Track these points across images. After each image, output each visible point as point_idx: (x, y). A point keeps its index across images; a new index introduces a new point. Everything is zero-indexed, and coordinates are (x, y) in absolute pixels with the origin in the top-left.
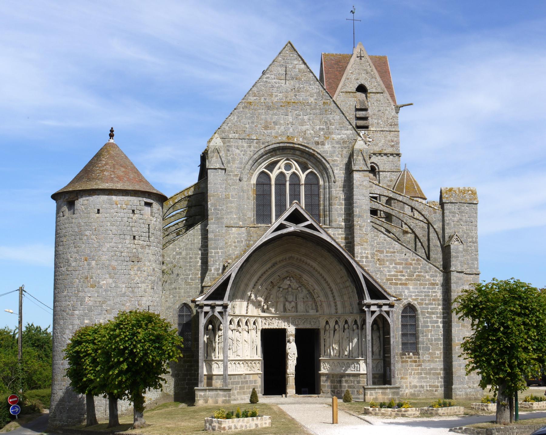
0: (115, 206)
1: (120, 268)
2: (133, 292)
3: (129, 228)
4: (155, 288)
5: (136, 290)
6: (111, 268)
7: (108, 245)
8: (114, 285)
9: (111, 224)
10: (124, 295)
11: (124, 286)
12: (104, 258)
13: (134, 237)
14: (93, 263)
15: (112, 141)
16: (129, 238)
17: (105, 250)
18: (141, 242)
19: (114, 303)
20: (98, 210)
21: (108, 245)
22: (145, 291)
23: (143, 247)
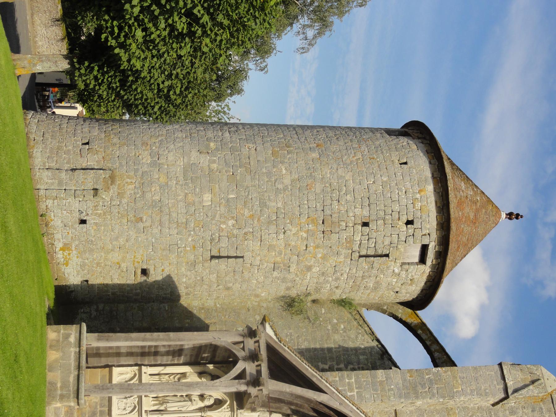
0: (416, 189)
1: (311, 197)
2: (269, 223)
3: (382, 213)
4: (275, 274)
5: (273, 228)
6: (310, 181)
7: (348, 176)
8: (280, 186)
9: (386, 182)
10: (263, 205)
11: (280, 205)
12: (327, 171)
13: (366, 224)
14: (315, 155)
15: (504, 216)
16: (363, 213)
17: (340, 172)
18: (358, 238)
19: (247, 187)
20: (406, 163)
21: (348, 176)
22: (271, 248)
23: (350, 241)
